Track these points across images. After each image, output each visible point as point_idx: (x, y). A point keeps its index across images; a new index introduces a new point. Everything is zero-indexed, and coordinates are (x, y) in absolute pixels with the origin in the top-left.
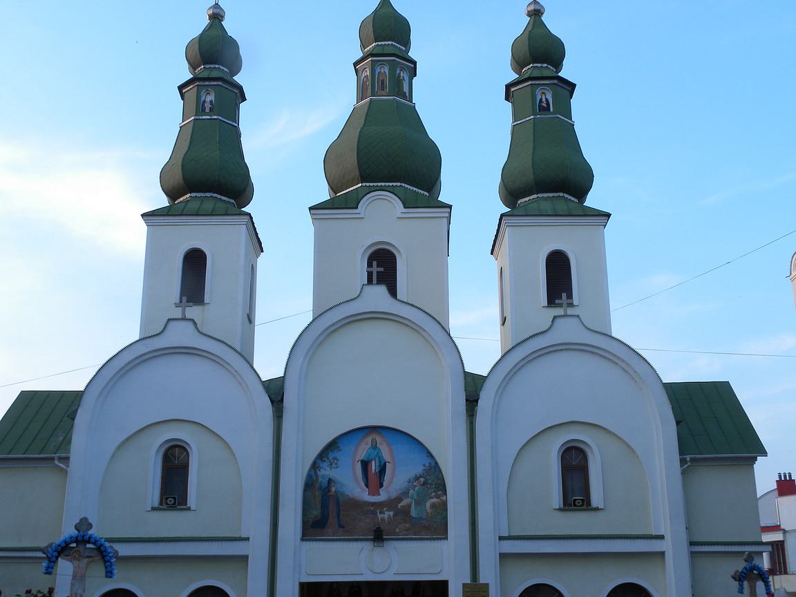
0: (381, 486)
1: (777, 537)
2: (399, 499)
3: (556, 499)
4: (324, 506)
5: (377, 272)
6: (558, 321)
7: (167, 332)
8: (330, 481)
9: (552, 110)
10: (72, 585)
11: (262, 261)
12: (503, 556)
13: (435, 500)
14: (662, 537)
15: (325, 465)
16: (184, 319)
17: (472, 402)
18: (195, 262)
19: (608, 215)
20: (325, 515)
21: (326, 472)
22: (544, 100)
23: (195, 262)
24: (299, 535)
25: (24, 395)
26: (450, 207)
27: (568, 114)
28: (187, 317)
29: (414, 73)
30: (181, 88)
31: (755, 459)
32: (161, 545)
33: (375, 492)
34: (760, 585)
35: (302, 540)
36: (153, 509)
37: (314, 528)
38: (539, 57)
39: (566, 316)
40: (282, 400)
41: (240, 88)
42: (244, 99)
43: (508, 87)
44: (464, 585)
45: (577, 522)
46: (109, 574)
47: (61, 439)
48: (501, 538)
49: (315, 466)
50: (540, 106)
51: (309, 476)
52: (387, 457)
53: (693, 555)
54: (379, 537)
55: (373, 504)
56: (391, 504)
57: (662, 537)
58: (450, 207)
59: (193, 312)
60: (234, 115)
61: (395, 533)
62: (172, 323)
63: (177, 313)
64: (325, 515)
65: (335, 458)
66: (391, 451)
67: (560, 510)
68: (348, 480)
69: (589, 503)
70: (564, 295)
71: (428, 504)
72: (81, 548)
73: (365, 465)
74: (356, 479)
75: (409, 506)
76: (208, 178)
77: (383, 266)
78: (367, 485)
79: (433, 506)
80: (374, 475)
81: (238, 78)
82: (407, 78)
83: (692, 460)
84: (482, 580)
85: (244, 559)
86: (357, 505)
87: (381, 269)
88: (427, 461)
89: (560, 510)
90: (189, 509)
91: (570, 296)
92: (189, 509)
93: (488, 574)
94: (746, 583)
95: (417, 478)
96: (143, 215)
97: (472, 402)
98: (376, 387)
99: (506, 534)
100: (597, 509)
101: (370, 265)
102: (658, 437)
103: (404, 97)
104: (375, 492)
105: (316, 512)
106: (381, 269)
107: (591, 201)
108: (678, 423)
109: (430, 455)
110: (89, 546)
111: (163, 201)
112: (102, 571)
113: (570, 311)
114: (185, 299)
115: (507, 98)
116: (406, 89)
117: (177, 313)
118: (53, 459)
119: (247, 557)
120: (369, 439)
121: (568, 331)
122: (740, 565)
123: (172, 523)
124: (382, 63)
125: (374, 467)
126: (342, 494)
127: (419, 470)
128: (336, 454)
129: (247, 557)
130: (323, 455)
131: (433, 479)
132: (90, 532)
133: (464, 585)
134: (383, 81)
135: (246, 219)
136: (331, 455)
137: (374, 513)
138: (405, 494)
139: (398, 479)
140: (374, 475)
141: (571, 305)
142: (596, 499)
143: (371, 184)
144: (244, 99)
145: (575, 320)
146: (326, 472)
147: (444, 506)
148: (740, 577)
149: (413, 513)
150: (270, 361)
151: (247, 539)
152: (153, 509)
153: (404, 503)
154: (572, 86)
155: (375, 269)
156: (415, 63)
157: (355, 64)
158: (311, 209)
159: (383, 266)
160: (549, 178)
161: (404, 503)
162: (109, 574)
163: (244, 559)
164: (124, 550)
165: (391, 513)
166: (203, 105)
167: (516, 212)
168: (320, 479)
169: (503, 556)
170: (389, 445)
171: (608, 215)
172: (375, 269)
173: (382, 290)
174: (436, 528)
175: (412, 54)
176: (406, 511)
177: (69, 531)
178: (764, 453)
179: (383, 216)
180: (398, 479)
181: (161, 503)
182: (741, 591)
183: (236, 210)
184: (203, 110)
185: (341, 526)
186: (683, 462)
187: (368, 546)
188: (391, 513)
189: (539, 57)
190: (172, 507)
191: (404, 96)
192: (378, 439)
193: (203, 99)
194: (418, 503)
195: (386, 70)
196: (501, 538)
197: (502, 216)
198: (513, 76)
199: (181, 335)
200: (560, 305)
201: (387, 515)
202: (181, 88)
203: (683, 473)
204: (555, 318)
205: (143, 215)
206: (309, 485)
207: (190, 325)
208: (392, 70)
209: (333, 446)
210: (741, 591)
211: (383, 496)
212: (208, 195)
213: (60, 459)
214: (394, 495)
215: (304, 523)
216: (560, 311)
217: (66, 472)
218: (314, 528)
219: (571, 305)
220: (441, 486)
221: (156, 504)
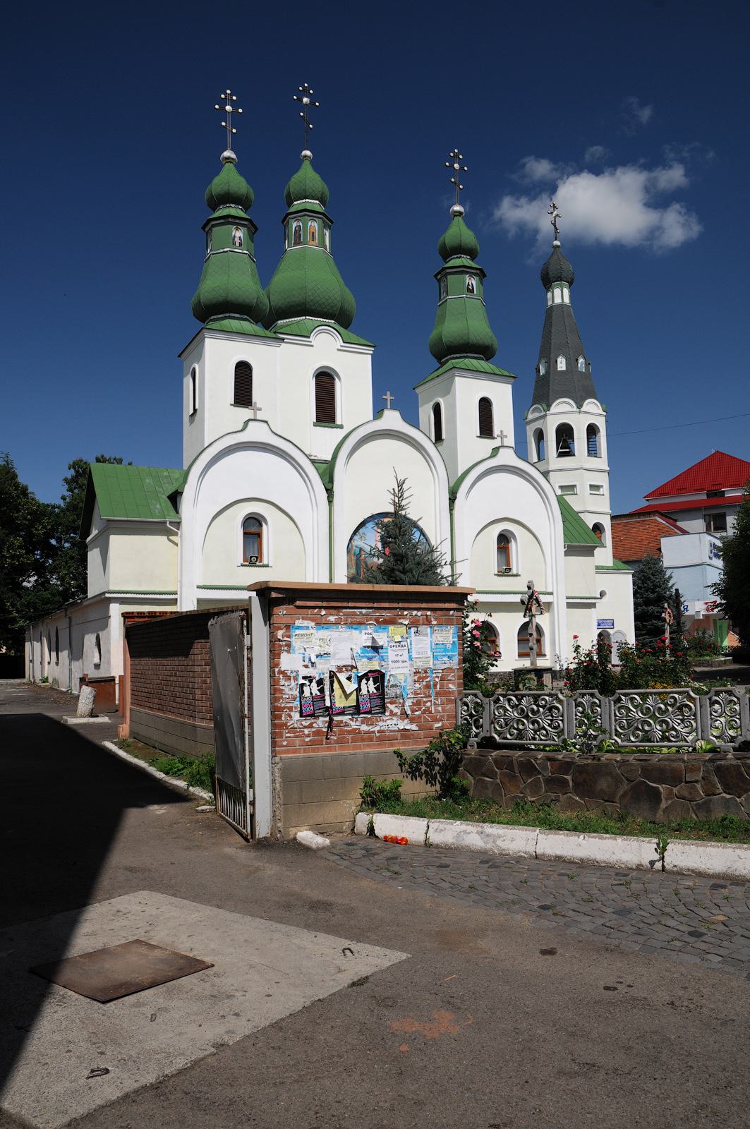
9: (475, 292)
14: (551, 594)
17: (452, 500)
21: (355, 543)
22: (470, 284)
28: (258, 418)
39: (502, 446)
50: (468, 288)
53: (567, 603)
57: (551, 594)
97: (452, 500)
112: (523, 614)
134: (313, 233)
143: (313, 318)
166: (234, 239)
168: (354, 548)
184: (234, 243)
193: (233, 234)
207: (265, 425)
213: (171, 523)
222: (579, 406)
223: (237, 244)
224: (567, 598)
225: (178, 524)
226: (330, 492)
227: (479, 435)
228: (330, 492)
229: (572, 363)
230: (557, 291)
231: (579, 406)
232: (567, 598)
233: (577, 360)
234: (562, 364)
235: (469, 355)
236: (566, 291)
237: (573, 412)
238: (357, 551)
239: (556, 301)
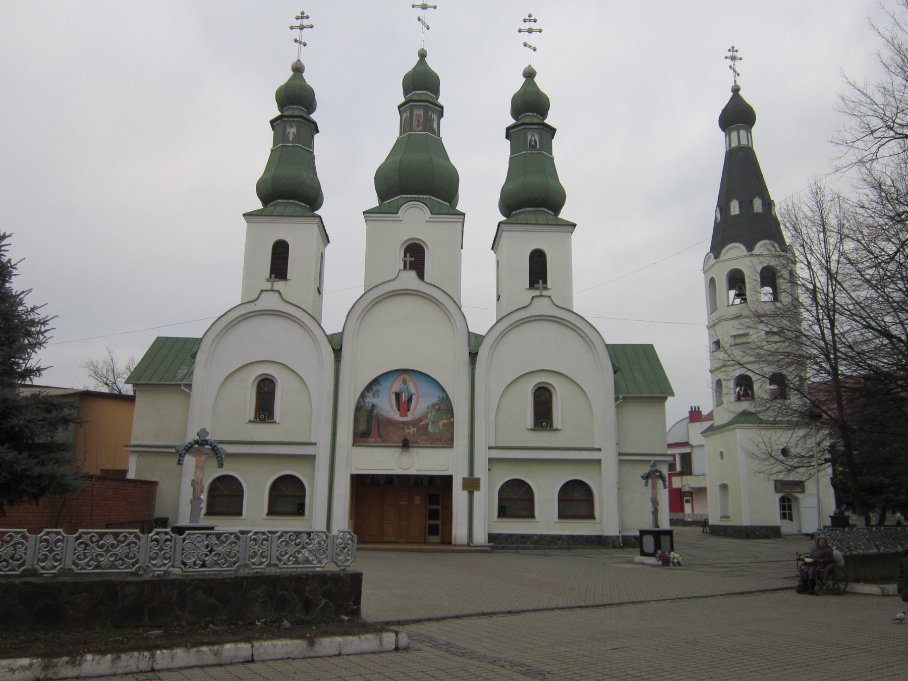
0: (409, 410)
1: (686, 450)
2: (420, 420)
3: (530, 422)
4: (369, 422)
5: (410, 262)
6: (535, 300)
7: (260, 299)
8: (373, 406)
10: (196, 472)
11: (329, 250)
12: (491, 460)
13: (445, 421)
14: (599, 450)
15: (370, 395)
16: (272, 290)
17: (473, 356)
18: (280, 251)
19: (574, 225)
20: (369, 428)
21: (370, 400)
23: (280, 251)
24: (351, 442)
25: (159, 339)
26: (464, 214)
27: (550, 151)
29: (441, 115)
30: (272, 122)
31: (666, 398)
32: (256, 446)
33: (404, 414)
34: (660, 483)
35: (353, 445)
36: (250, 422)
37: (361, 437)
38: (530, 108)
39: (541, 296)
40: (340, 350)
41: (315, 124)
42: (317, 131)
43: (508, 129)
44: (464, 479)
45: (543, 438)
46: (221, 465)
47: (186, 371)
48: (490, 448)
49: (363, 396)
51: (359, 402)
52: (413, 390)
53: (620, 461)
54: (406, 445)
55: (403, 422)
56: (416, 422)
57: (599, 450)
58: (464, 214)
59: (279, 285)
60: (310, 143)
61: (417, 443)
62: (264, 294)
63: (268, 286)
64: (369, 428)
65: (377, 391)
66: (416, 387)
67: (531, 430)
68: (386, 406)
69: (551, 426)
70: (541, 281)
71: (441, 424)
72: (201, 448)
73: (398, 395)
74: (392, 406)
75: (427, 424)
76: (290, 190)
77: (415, 256)
78: (399, 410)
79: (444, 424)
80: (403, 403)
81: (313, 116)
82: (436, 119)
83: (624, 398)
84: (476, 476)
85: (313, 457)
86: (391, 422)
87: (413, 259)
88: (440, 394)
89: (531, 430)
90: (275, 422)
91: (545, 282)
92: (275, 422)
93: (481, 472)
94: (650, 481)
95: (433, 406)
96: (244, 215)
97: (473, 356)
98: (407, 341)
99: (493, 445)
100: (557, 430)
101: (405, 256)
102: (600, 382)
103: (433, 132)
104: (404, 414)
105: (363, 427)
106: (413, 259)
107: (564, 215)
108: (615, 372)
109: (443, 390)
110: (206, 446)
111: (257, 204)
112: (216, 464)
113: (544, 293)
114: (273, 276)
115: (507, 137)
116: (435, 127)
117: (268, 286)
118: (180, 385)
119: (314, 456)
120: (401, 378)
121: (542, 307)
122: (646, 469)
123: (263, 432)
124: (419, 107)
125: (404, 397)
126: (382, 416)
127: (435, 400)
128: (378, 388)
129: (314, 456)
130: (369, 388)
131: (445, 407)
132: (207, 438)
133: (464, 479)
135: (318, 220)
136: (374, 388)
137: (403, 429)
138: (426, 416)
139: (421, 406)
140: (403, 403)
141: (546, 288)
142: (556, 423)
144: (317, 131)
145: (547, 299)
146: (370, 400)
147: (451, 425)
148: (646, 477)
149: (431, 429)
150: (333, 322)
151: (315, 444)
152: (250, 422)
153: (424, 422)
154: (552, 131)
155: (408, 259)
156: (442, 108)
157: (399, 107)
158: (364, 213)
159: (415, 256)
160: (533, 198)
161: (424, 422)
162: (221, 465)
163: (313, 457)
164: (230, 449)
165: (415, 429)
167: (510, 221)
169: (491, 460)
170: (414, 383)
171: (574, 225)
172: (408, 259)
173: (413, 274)
174: (446, 440)
175: (441, 101)
176: (426, 427)
177: (192, 436)
178: (672, 394)
179: (415, 221)
180: (421, 406)
181: (255, 418)
182: (646, 485)
183: (310, 214)
185: (380, 437)
186: (617, 399)
187: (398, 450)
188: (415, 429)
189: (530, 108)
190: (263, 421)
191: (433, 132)
192: (407, 378)
194: (433, 423)
195: (421, 112)
196: (490, 448)
197: (500, 223)
198: (512, 121)
199: (270, 302)
200: (538, 289)
201: (412, 430)
202: (272, 122)
203: (617, 407)
204: (533, 297)
205: (244, 215)
206: (358, 409)
207: (277, 294)
208: (426, 114)
209: (376, 381)
210: (646, 485)
211: (409, 418)
212: (291, 201)
214: (417, 417)
215: (355, 434)
216: (537, 293)
217: (189, 395)
218: (361, 437)
219: (546, 288)
220: (450, 411)
221: (252, 418)
222: (750, 247)
224: (620, 454)
225: (189, 386)
226: (338, 352)
227: (528, 287)
228: (338, 352)
229: (746, 205)
230: (734, 135)
231: (750, 247)
232: (620, 454)
233: (752, 202)
234: (735, 208)
235: (528, 209)
236: (743, 133)
237: (745, 256)
238: (369, 408)
239: (733, 145)
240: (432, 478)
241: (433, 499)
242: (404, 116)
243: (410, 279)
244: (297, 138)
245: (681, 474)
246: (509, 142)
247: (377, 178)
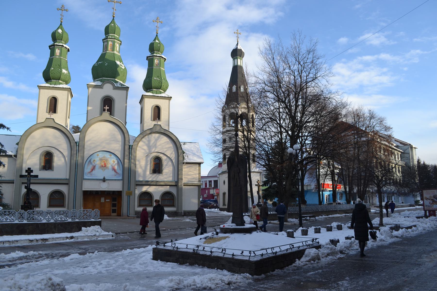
1: (216, 179)
19: (171, 97)
30: (50, 47)
59: (54, 116)
63: (48, 116)
117: (48, 116)
155: (107, 108)
171: (171, 97)
172: (107, 108)
190: (46, 170)
223: (58, 55)
230: (236, 60)
240: (114, 192)
241: (114, 200)
242: (105, 44)
243: (106, 115)
244: (61, 53)
245: (213, 188)
246: (147, 61)
247: (92, 69)
